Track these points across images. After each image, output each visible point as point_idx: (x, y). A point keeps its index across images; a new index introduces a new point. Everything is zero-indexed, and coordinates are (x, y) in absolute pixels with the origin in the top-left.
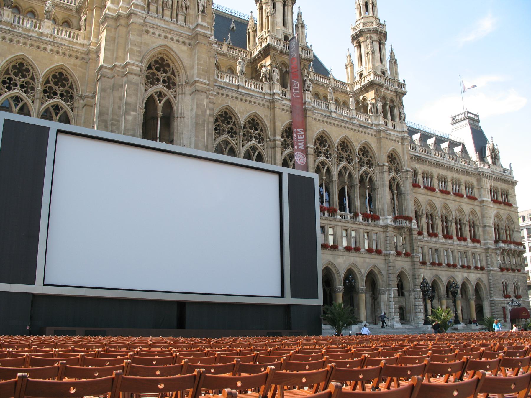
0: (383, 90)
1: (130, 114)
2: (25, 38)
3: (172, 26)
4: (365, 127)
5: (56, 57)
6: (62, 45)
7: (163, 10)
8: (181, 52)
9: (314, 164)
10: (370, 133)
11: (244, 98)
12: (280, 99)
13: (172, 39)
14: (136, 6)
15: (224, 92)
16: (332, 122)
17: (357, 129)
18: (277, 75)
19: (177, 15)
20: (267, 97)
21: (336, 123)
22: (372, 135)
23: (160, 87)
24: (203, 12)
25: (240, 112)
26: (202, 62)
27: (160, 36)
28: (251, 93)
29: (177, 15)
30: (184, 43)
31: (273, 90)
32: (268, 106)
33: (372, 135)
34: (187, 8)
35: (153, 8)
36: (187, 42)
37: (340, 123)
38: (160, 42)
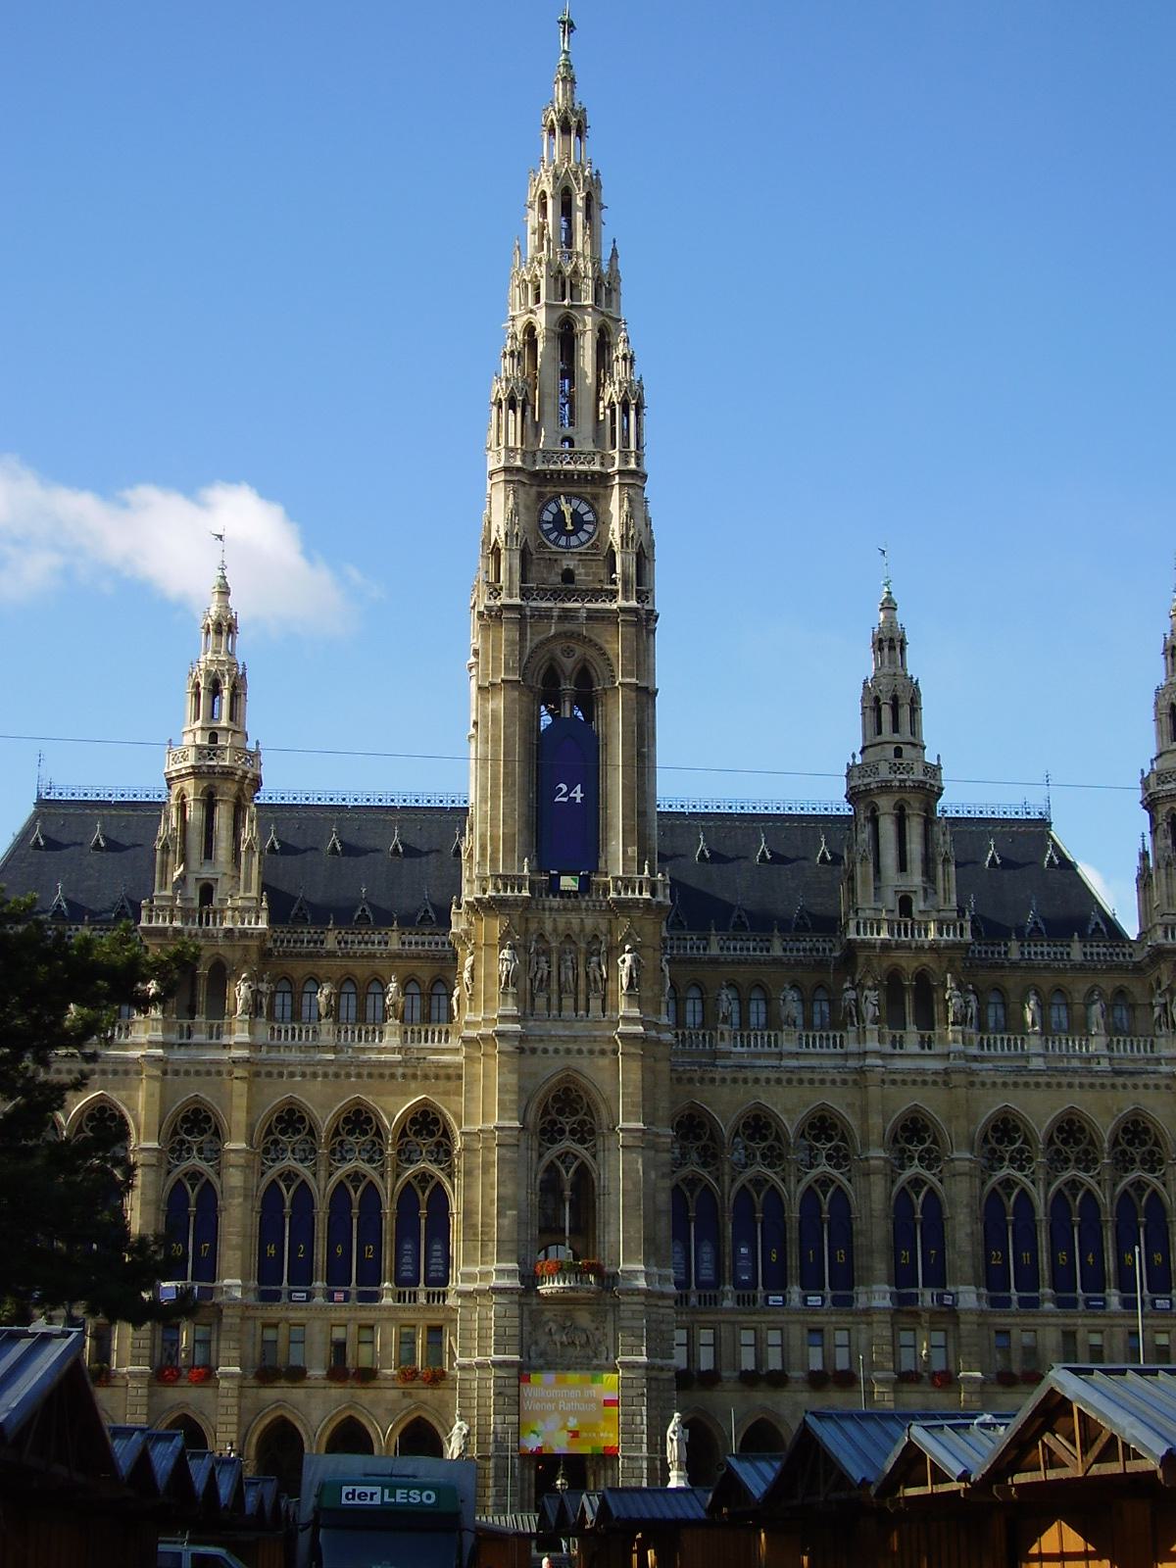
1: (505, 1216)
2: (358, 1066)
3: (579, 1029)
4: (1132, 1074)
5: (413, 1085)
9: (982, 1189)
10: (1151, 1083)
11: (791, 1079)
12: (879, 1062)
13: (580, 1052)
14: (503, 1018)
15: (750, 1075)
16: (1032, 1080)
17: (1107, 1081)
18: (871, 1008)
20: (852, 1063)
21: (1042, 1080)
22: (1157, 1087)
23: (567, 1144)
24: (631, 986)
26: (630, 1090)
27: (556, 1051)
28: (814, 1062)
29: (588, 1000)
30: (603, 1052)
31: (865, 1042)
33: (1157, 1087)
34: (607, 980)
35: (541, 1002)
37: (1055, 1077)
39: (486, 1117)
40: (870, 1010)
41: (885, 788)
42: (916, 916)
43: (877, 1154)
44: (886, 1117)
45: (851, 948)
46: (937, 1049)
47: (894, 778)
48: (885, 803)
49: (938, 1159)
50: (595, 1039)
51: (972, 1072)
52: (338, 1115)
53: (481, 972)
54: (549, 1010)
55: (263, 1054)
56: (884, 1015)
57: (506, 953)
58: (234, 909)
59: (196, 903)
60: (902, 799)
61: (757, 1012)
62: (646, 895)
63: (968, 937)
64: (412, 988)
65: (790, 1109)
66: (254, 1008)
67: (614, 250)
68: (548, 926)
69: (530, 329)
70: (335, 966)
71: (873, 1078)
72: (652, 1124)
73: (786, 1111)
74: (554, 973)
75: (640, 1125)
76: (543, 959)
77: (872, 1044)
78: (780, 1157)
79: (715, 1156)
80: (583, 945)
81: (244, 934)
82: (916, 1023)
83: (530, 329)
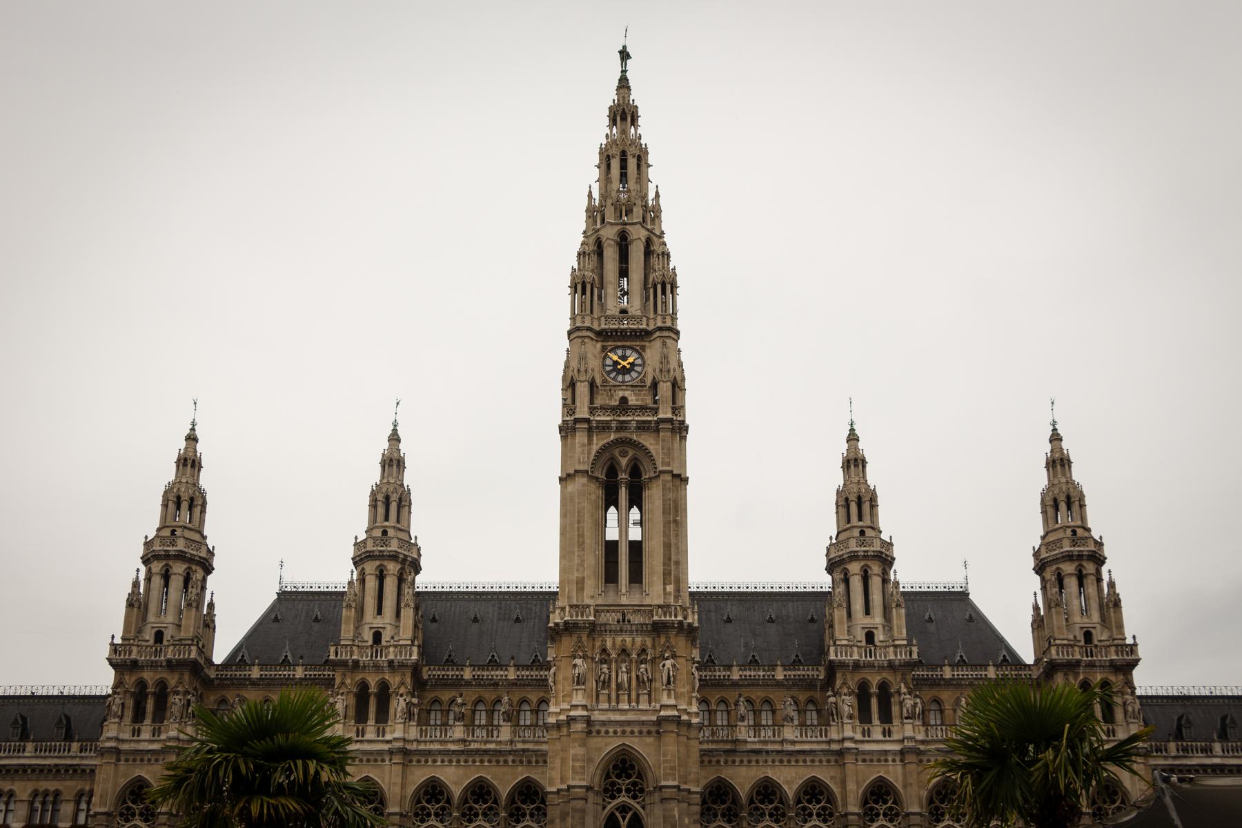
0: (1081, 670)
3: (631, 717)
6: (524, 750)
7: (618, 696)
8: (643, 747)
12: (853, 745)
13: (632, 732)
14: (575, 707)
15: (761, 758)
18: (846, 708)
19: (638, 695)
20: (835, 747)
24: (669, 682)
25: (787, 782)
28: (807, 747)
30: (649, 733)
32: (836, 761)
34: (650, 681)
36: (653, 729)
38: (616, 742)
39: (563, 780)
40: (846, 709)
41: (854, 557)
42: (877, 643)
43: (854, 808)
44: (858, 783)
45: (832, 668)
46: (895, 737)
47: (860, 548)
48: (855, 568)
49: (897, 815)
50: (643, 723)
51: (919, 753)
52: (466, 790)
53: (560, 677)
54: (609, 702)
55: (414, 747)
56: (856, 714)
57: (579, 661)
58: (396, 646)
59: (370, 643)
60: (866, 565)
61: (766, 718)
62: (680, 618)
63: (915, 656)
64: (525, 707)
65: (790, 779)
66: (409, 715)
67: (657, 195)
68: (609, 644)
69: (599, 245)
70: (471, 695)
71: (849, 759)
72: (685, 783)
73: (787, 782)
74: (613, 674)
75: (676, 783)
76: (605, 666)
77: (848, 733)
78: (784, 815)
79: (736, 815)
80: (634, 656)
81: (402, 665)
82: (880, 719)
83: (599, 245)
